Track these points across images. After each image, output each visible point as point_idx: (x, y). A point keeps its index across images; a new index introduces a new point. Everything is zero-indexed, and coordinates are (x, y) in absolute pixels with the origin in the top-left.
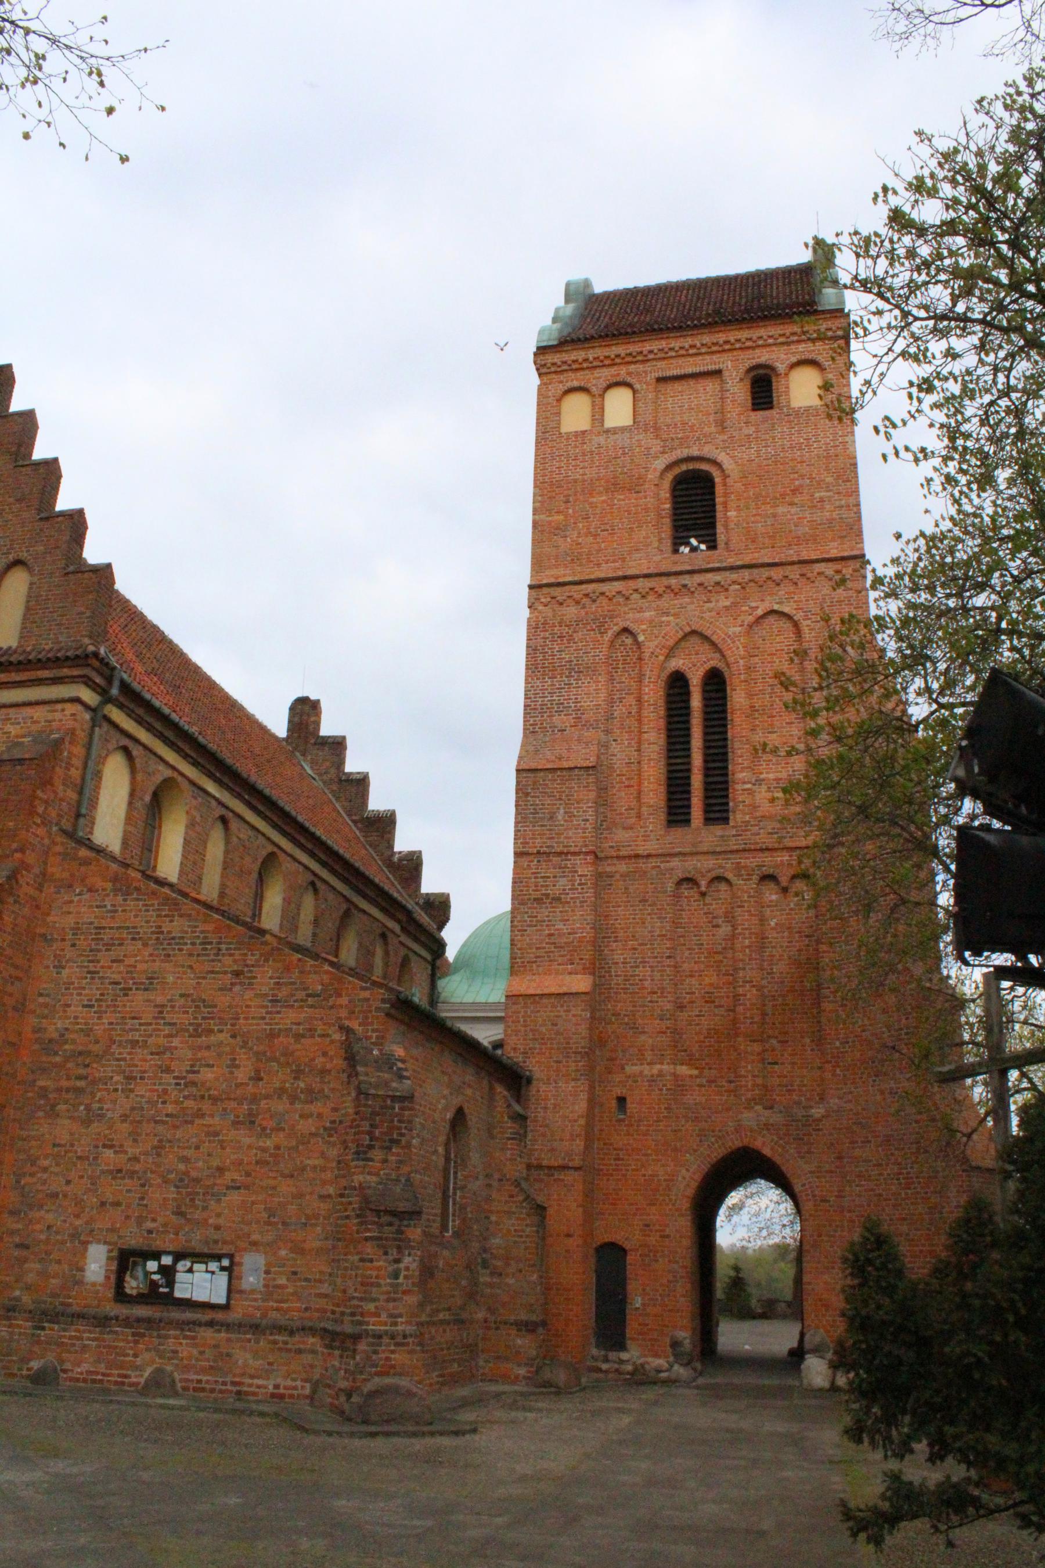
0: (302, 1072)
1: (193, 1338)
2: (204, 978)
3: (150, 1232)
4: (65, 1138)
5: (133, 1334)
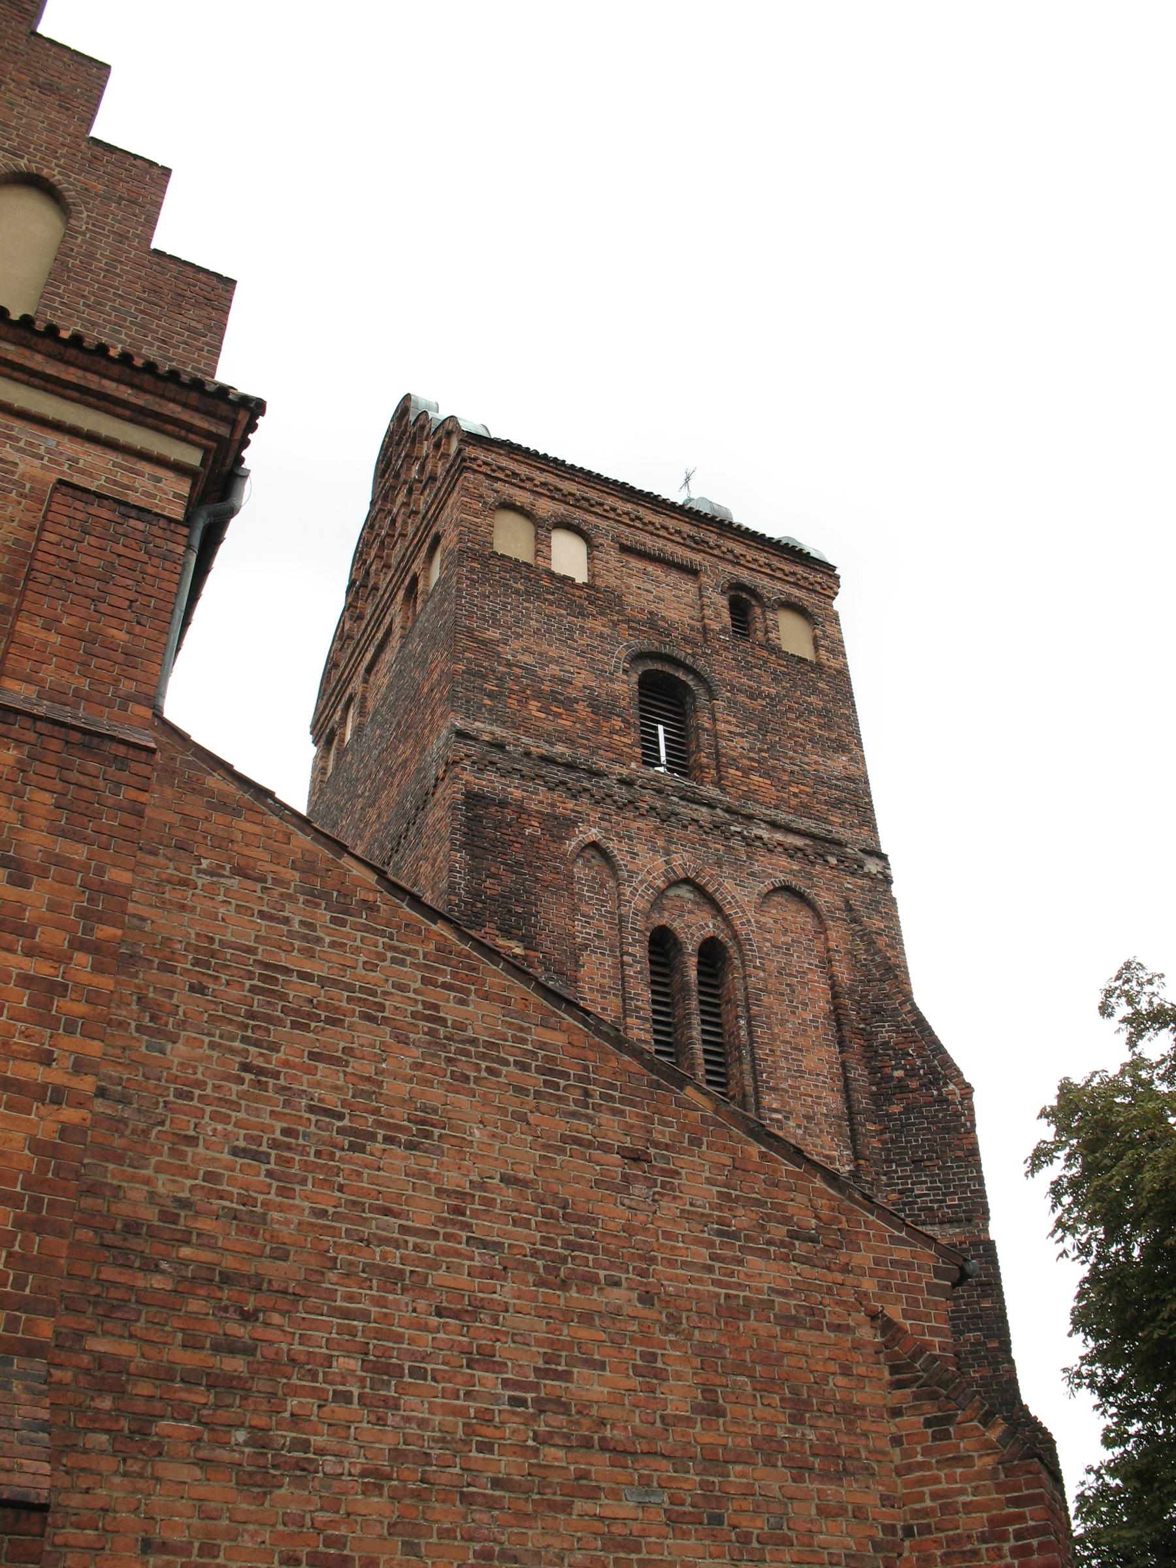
2: (561, 1151)
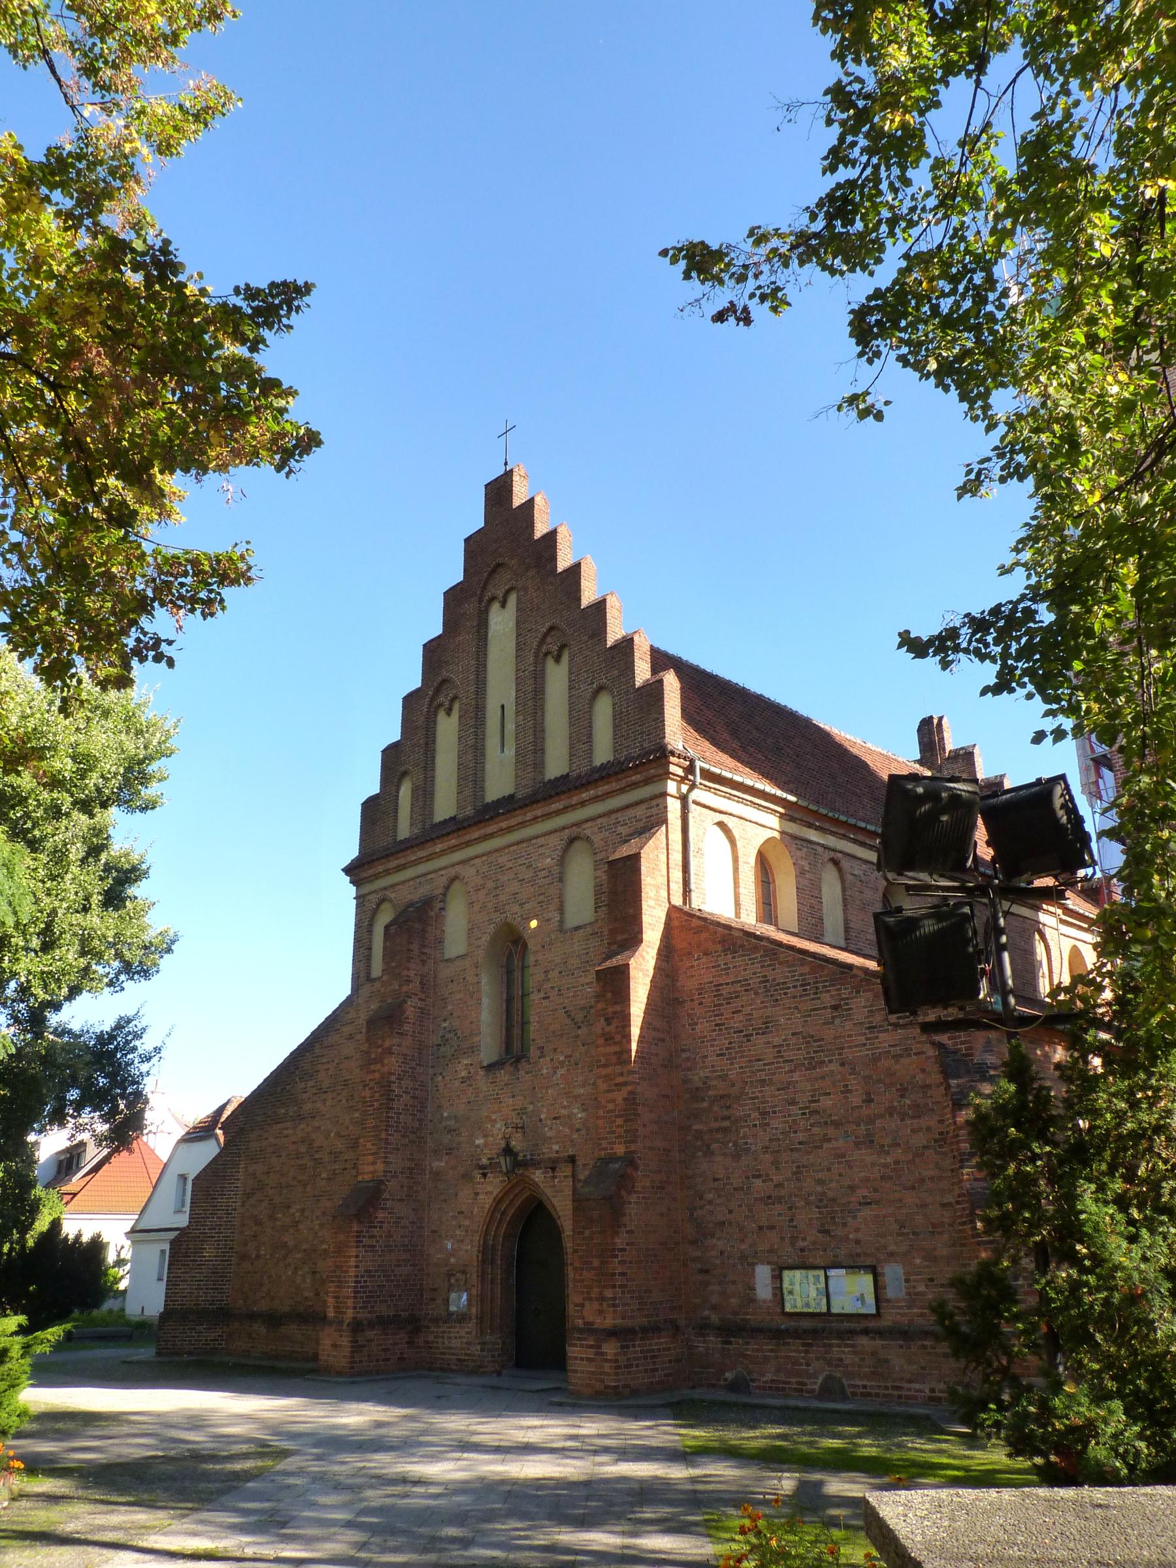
0: (906, 1089)
1: (853, 1346)
3: (802, 1250)
5: (804, 1345)
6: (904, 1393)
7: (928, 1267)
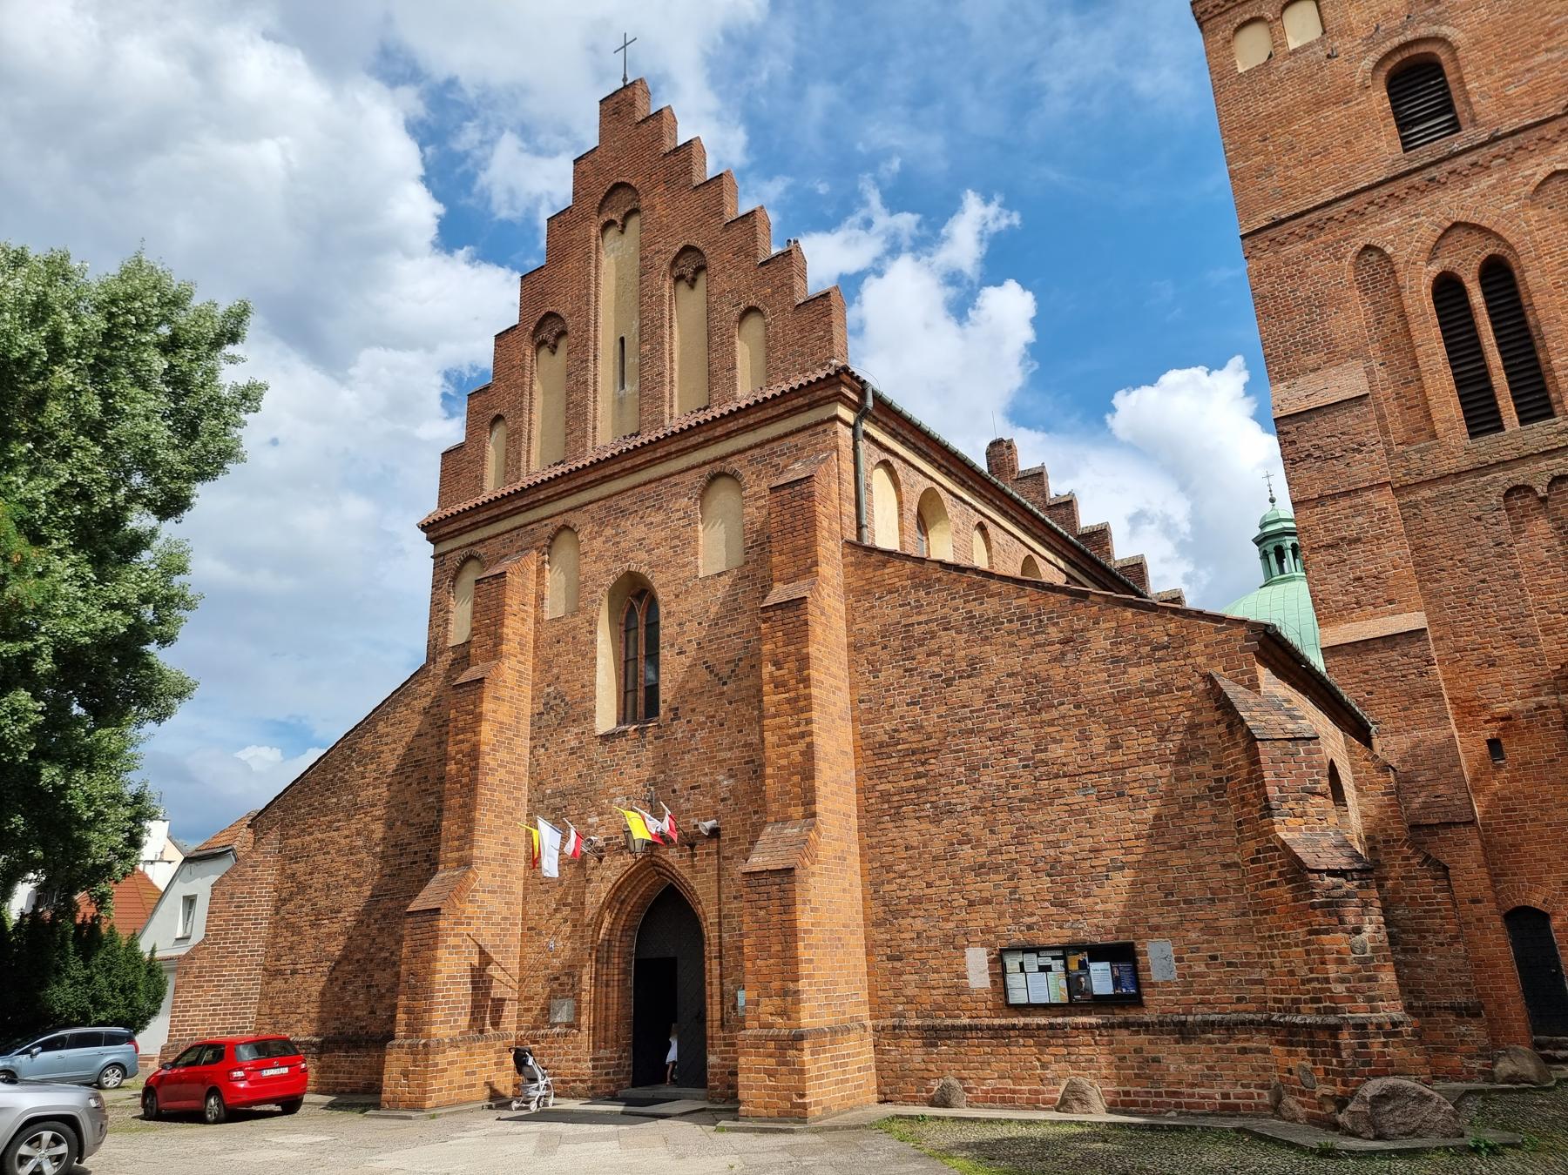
3: (1030, 928)
4: (915, 840)
6: (1184, 1100)
7: (1208, 942)
